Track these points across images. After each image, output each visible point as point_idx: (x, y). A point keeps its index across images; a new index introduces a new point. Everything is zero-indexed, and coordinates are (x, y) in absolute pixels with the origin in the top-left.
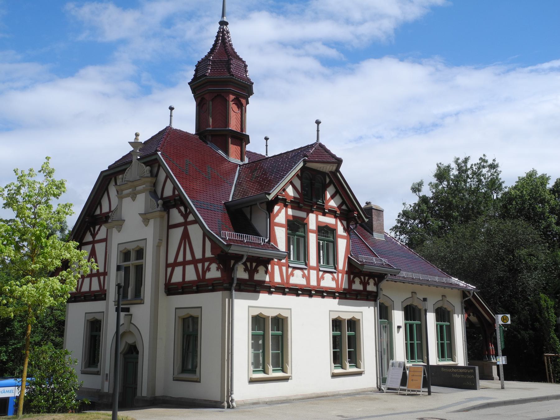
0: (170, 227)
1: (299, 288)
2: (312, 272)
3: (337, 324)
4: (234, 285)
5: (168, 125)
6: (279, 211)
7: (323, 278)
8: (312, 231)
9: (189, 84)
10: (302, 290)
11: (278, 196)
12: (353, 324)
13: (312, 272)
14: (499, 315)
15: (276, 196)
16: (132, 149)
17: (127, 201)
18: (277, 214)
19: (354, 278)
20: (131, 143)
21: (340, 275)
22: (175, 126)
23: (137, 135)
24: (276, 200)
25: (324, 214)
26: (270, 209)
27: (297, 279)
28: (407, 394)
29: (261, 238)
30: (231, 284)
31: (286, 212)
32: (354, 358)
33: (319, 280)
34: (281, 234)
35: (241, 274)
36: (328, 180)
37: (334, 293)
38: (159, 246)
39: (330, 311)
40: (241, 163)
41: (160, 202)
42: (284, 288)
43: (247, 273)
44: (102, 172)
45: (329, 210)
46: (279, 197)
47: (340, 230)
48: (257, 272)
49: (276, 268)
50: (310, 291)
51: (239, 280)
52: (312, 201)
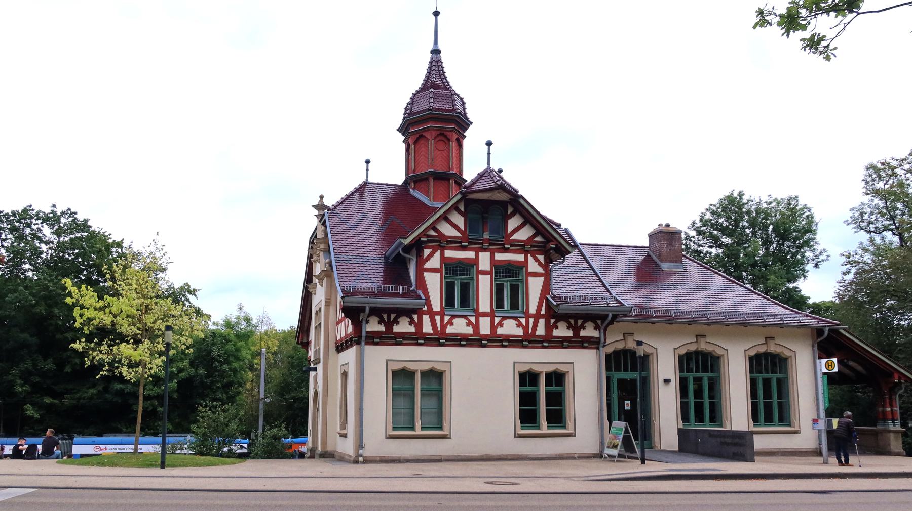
1: (462, 338)
2: (481, 318)
3: (527, 378)
4: (363, 339)
6: (431, 255)
7: (501, 324)
9: (398, 130)
10: (468, 340)
11: (420, 238)
12: (557, 378)
14: (822, 360)
15: (417, 239)
16: (316, 212)
18: (428, 258)
19: (555, 323)
20: (314, 207)
21: (531, 321)
22: (370, 180)
23: (322, 197)
25: (506, 251)
27: (460, 327)
28: (578, 457)
29: (401, 287)
30: (360, 337)
31: (442, 254)
32: (557, 417)
33: (493, 327)
34: (434, 283)
35: (374, 326)
36: (510, 210)
37: (522, 341)
39: (515, 363)
42: (438, 339)
43: (383, 325)
45: (511, 245)
46: (422, 239)
47: (533, 267)
48: (398, 323)
49: (426, 318)
50: (481, 340)
51: (367, 332)
52: (483, 237)
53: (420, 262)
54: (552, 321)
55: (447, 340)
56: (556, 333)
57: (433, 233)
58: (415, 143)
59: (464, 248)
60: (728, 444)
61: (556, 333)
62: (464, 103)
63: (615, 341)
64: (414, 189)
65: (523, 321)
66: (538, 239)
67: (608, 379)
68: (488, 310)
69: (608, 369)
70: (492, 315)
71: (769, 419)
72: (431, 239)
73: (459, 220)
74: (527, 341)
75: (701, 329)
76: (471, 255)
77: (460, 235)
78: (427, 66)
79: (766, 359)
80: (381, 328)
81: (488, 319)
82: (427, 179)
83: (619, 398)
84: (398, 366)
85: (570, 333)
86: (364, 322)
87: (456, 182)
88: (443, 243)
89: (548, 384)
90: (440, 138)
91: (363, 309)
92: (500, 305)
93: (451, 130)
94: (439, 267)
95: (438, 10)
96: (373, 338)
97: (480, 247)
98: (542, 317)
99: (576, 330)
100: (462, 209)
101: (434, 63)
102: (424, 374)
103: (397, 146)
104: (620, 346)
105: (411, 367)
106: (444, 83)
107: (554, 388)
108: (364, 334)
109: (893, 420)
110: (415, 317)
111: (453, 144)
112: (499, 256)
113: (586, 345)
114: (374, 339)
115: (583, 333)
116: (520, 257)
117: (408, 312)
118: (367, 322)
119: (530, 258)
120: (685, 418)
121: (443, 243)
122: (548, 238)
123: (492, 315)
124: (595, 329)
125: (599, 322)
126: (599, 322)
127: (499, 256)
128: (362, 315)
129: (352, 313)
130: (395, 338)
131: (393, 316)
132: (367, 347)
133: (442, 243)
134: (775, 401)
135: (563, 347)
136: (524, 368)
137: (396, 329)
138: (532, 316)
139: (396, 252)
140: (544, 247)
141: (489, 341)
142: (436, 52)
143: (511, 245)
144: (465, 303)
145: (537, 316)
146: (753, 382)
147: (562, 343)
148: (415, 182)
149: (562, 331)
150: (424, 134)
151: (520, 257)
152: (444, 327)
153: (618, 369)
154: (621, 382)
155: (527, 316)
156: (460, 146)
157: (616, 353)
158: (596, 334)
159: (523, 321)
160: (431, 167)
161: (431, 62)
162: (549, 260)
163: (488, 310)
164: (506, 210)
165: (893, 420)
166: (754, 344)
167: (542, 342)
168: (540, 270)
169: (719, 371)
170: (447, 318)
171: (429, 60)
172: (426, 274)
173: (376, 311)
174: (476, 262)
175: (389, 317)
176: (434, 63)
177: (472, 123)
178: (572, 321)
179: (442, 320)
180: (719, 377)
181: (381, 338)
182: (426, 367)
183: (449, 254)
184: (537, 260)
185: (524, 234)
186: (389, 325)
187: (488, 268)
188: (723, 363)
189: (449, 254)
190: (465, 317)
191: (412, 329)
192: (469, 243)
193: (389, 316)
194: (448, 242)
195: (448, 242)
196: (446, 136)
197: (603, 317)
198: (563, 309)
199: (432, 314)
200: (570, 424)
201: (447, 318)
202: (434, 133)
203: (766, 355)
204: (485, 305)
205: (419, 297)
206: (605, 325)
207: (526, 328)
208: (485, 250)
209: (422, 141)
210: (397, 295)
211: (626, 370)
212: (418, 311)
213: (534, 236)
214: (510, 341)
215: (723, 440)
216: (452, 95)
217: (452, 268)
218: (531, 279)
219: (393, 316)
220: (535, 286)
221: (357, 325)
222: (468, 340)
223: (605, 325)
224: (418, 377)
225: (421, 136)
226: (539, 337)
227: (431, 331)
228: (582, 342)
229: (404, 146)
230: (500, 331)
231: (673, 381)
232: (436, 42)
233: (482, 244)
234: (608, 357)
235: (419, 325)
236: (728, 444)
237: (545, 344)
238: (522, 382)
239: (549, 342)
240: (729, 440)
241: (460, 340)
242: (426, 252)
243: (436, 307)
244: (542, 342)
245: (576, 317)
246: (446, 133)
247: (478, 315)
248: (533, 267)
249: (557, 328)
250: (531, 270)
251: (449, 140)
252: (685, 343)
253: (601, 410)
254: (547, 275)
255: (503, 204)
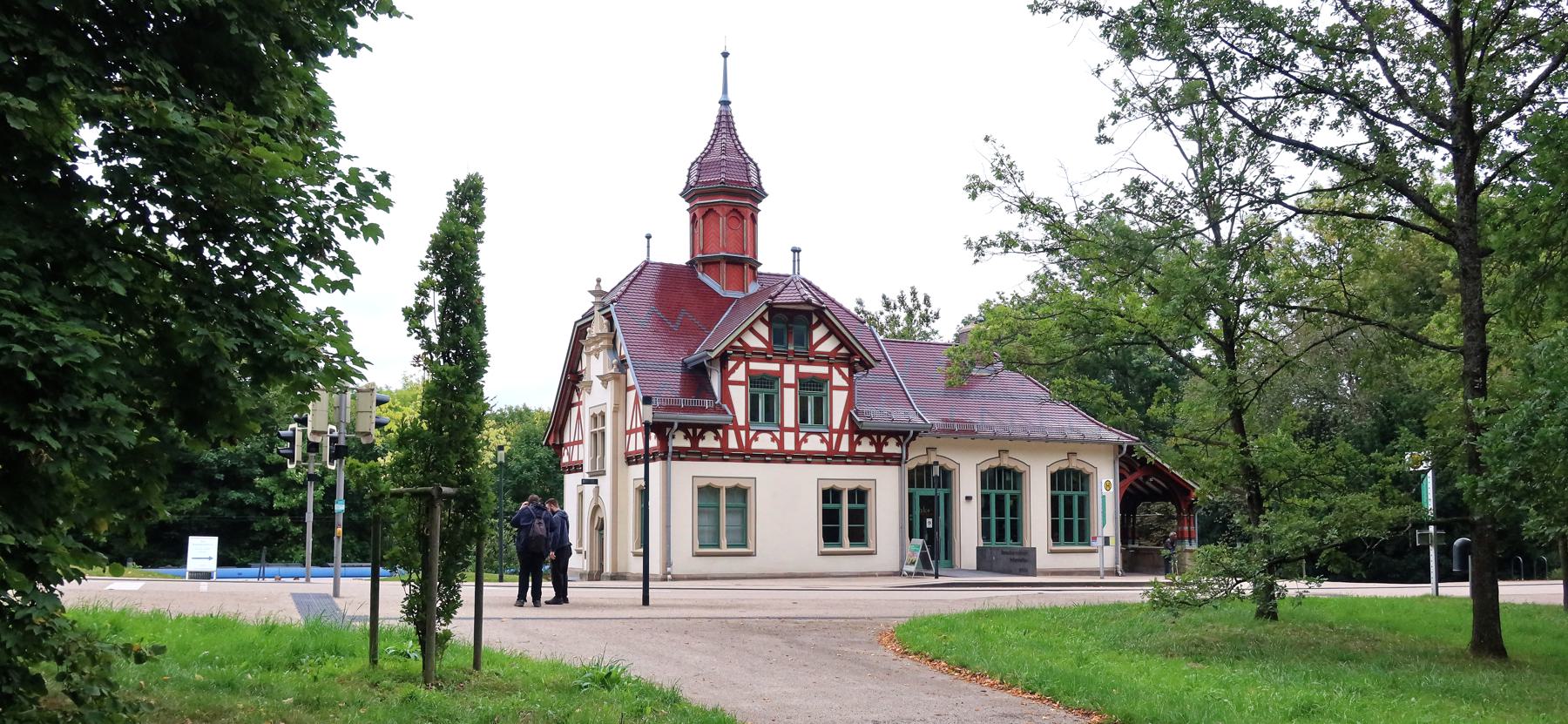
0: (628, 389)
2: (786, 434)
3: (830, 495)
4: (670, 454)
5: (645, 259)
6: (736, 367)
7: (805, 440)
8: (789, 386)
10: (772, 456)
12: (859, 495)
13: (786, 434)
16: (593, 298)
17: (593, 357)
19: (859, 438)
21: (835, 436)
22: (653, 259)
23: (599, 281)
24: (723, 358)
25: (810, 363)
26: (724, 365)
27: (764, 443)
30: (667, 453)
31: (747, 366)
33: (798, 443)
34: (739, 395)
35: (680, 441)
36: (815, 320)
37: (825, 458)
38: (616, 411)
40: (739, 295)
41: (615, 361)
44: (576, 323)
45: (816, 357)
47: (838, 380)
48: (703, 438)
50: (785, 456)
51: (674, 448)
53: (725, 374)
54: (856, 436)
55: (752, 455)
56: (859, 449)
57: (738, 344)
58: (704, 217)
59: (769, 360)
60: (1016, 561)
61: (859, 449)
62: (758, 170)
63: (917, 456)
64: (703, 272)
65: (827, 436)
66: (843, 350)
67: (911, 495)
68: (793, 425)
69: (911, 485)
70: (796, 430)
71: (1069, 538)
72: (736, 351)
73: (763, 330)
74: (831, 457)
75: (1005, 444)
76: (775, 367)
77: (764, 346)
78: (715, 120)
79: (1068, 476)
80: (687, 444)
81: (792, 435)
82: (719, 263)
83: (921, 516)
84: (704, 483)
85: (872, 449)
86: (670, 437)
87: (750, 267)
88: (748, 355)
89: (851, 501)
90: (732, 214)
91: (671, 425)
92: (804, 419)
93: (745, 206)
94: (743, 379)
95: (728, 51)
96: (679, 453)
97: (785, 358)
98: (846, 432)
99: (879, 446)
100: (767, 318)
101: (723, 119)
102: (728, 490)
103: (680, 213)
104: (923, 461)
105: (716, 483)
106: (736, 146)
107: (856, 506)
108: (670, 450)
109: (1190, 539)
110: (720, 432)
111: (747, 222)
112: (804, 369)
113: (888, 461)
114: (680, 455)
115: (886, 450)
116: (824, 370)
117: (713, 428)
118: (673, 437)
119: (835, 372)
120: (986, 533)
121: (748, 355)
122: (853, 351)
123: (796, 430)
124: (897, 445)
125: (901, 438)
126: (901, 438)
127: (804, 369)
128: (668, 430)
129: (658, 428)
130: (701, 454)
131: (699, 431)
132: (674, 464)
133: (746, 354)
134: (1076, 519)
135: (866, 464)
136: (827, 485)
137: (702, 444)
138: (836, 431)
139: (701, 361)
140: (849, 359)
141: (793, 457)
142: (725, 103)
143: (816, 357)
144: (769, 417)
145: (841, 432)
146: (1054, 501)
147: (865, 459)
148: (704, 264)
149: (865, 447)
150: (715, 208)
151: (824, 370)
152: (749, 442)
153: (921, 486)
154: (921, 497)
155: (832, 431)
156: (754, 220)
157: (919, 468)
158: (898, 450)
159: (827, 436)
160: (724, 249)
161: (720, 117)
162: (853, 371)
163: (793, 425)
164: (811, 320)
165: (1190, 539)
166: (1058, 461)
167: (845, 458)
168: (845, 384)
169: (1021, 489)
170: (752, 434)
171: (717, 113)
172: (730, 387)
173: (683, 427)
174: (781, 373)
175: (694, 432)
176: (723, 119)
177: (767, 195)
178: (875, 437)
179: (747, 435)
180: (1021, 494)
181: (687, 454)
182: (731, 484)
183: (754, 366)
184: (841, 373)
185: (829, 346)
186: (695, 440)
187: (792, 381)
188: (1025, 479)
189: (754, 366)
190: (770, 432)
191: (717, 445)
192: (774, 355)
193: (694, 431)
194: (753, 353)
195: (753, 353)
196: (739, 213)
197: (906, 434)
198: (867, 426)
199: (737, 429)
200: (871, 541)
201: (752, 434)
202: (727, 209)
203: (1069, 471)
204: (790, 420)
205: (725, 412)
206: (907, 441)
207: (829, 444)
208: (789, 362)
209: (711, 216)
210: (702, 410)
211: (929, 486)
212: (725, 427)
213: (839, 348)
214: (813, 457)
215: (1012, 557)
216: (746, 162)
217: (757, 381)
218: (835, 393)
219: (699, 431)
220: (839, 400)
221: (664, 440)
222: (772, 456)
223: (907, 441)
224: (723, 494)
225: (710, 210)
226: (842, 453)
227: (736, 447)
228: (885, 459)
229: (687, 217)
230: (804, 447)
231: (974, 499)
232: (725, 91)
233: (786, 356)
234: (911, 472)
235: (725, 441)
236: (1016, 561)
237: (848, 460)
238: (825, 500)
239: (852, 458)
240: (1016, 557)
241: (764, 456)
242: (731, 364)
243: (741, 422)
244: (845, 458)
245: (879, 433)
246: (740, 209)
247: (783, 430)
248: (838, 380)
249: (860, 444)
250: (835, 383)
251: (743, 217)
252: (987, 458)
253: (901, 528)
254: (850, 389)
255: (808, 314)
